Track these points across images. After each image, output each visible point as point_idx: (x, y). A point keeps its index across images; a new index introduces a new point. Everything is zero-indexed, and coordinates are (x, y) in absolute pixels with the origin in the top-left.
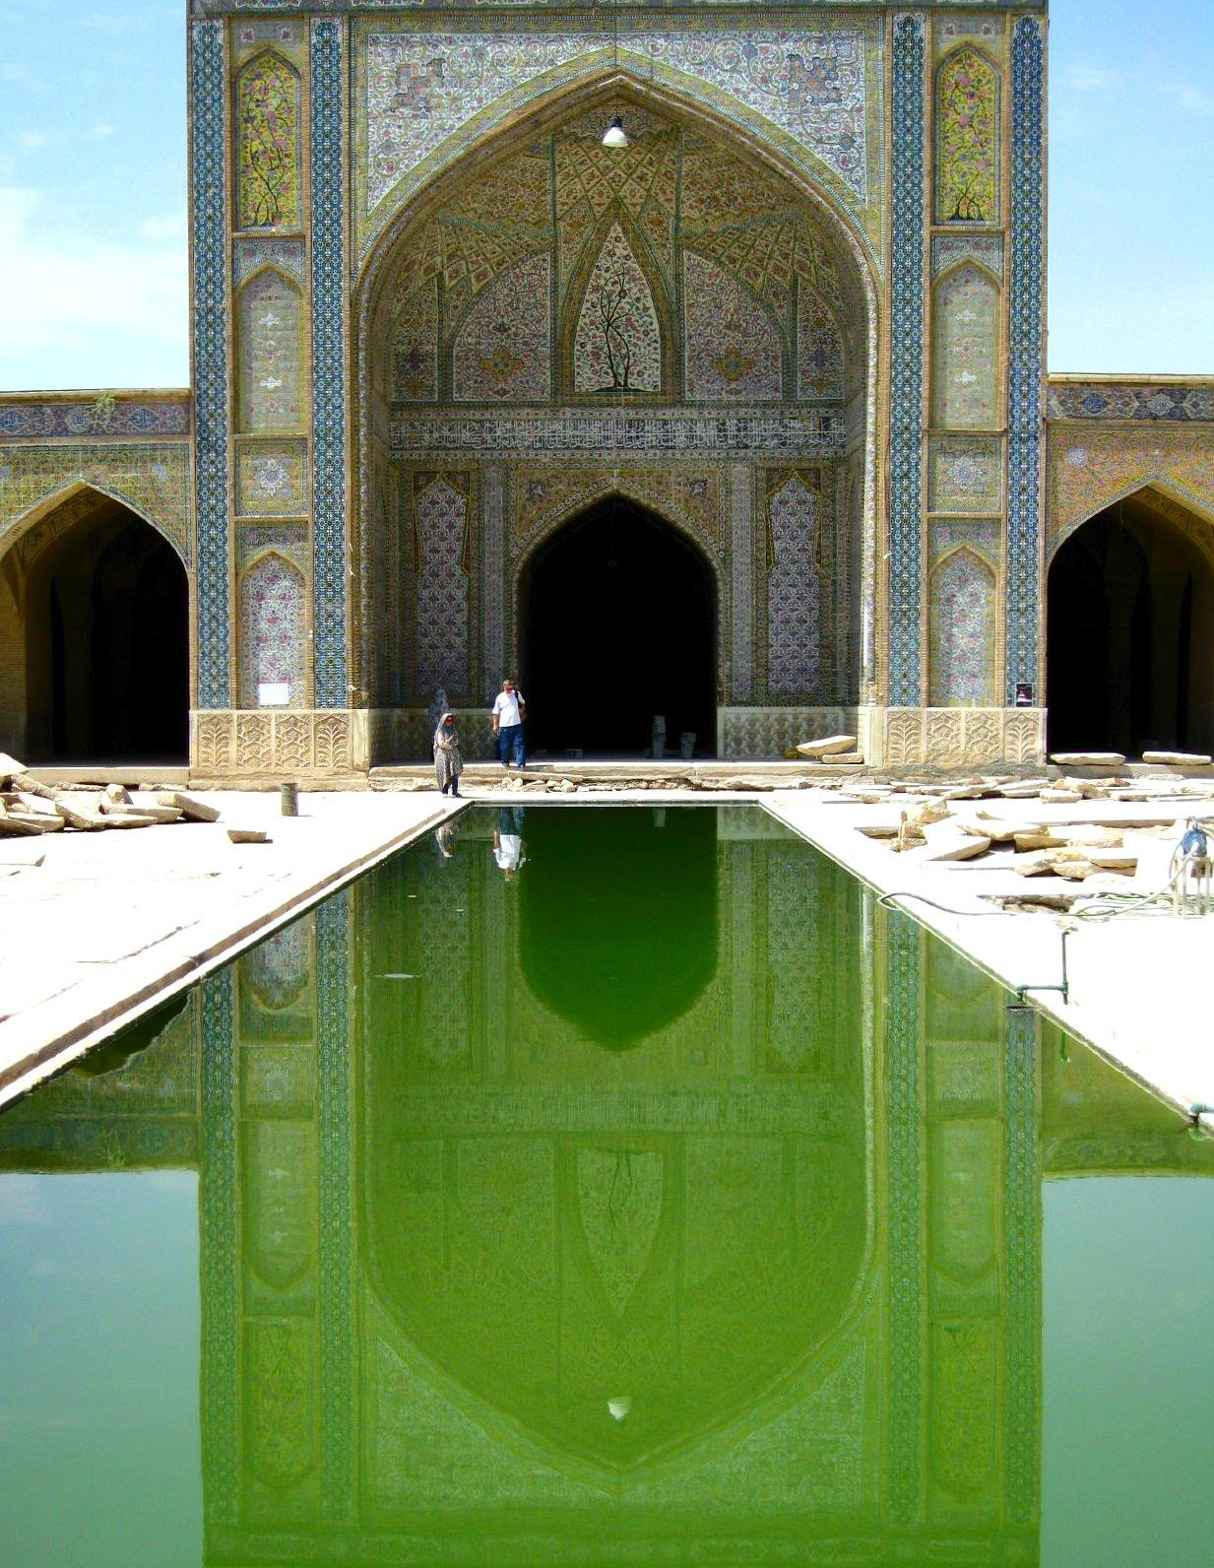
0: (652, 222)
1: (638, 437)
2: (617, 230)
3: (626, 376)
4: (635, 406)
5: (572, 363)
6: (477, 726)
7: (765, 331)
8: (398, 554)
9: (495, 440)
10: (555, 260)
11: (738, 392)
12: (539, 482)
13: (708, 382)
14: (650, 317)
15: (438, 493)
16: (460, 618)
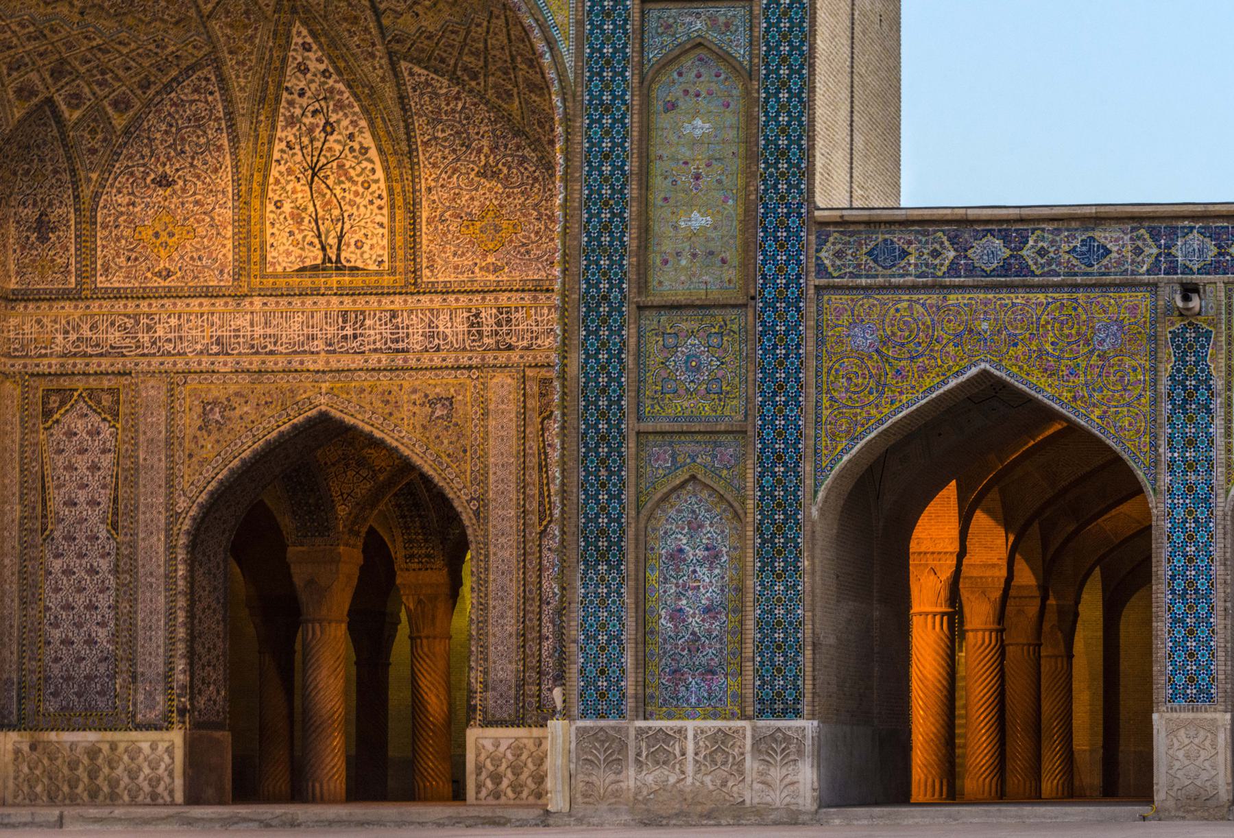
0: (345, 19)
1: (355, 337)
2: (300, 34)
3: (339, 249)
4: (353, 293)
5: (262, 231)
6: (126, 758)
7: (536, 180)
8: (17, 507)
9: (154, 343)
10: (222, 79)
11: (497, 269)
12: (215, 402)
13: (455, 254)
14: (372, 161)
15: (78, 421)
16: (104, 601)
